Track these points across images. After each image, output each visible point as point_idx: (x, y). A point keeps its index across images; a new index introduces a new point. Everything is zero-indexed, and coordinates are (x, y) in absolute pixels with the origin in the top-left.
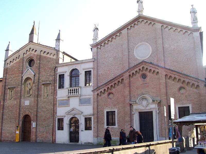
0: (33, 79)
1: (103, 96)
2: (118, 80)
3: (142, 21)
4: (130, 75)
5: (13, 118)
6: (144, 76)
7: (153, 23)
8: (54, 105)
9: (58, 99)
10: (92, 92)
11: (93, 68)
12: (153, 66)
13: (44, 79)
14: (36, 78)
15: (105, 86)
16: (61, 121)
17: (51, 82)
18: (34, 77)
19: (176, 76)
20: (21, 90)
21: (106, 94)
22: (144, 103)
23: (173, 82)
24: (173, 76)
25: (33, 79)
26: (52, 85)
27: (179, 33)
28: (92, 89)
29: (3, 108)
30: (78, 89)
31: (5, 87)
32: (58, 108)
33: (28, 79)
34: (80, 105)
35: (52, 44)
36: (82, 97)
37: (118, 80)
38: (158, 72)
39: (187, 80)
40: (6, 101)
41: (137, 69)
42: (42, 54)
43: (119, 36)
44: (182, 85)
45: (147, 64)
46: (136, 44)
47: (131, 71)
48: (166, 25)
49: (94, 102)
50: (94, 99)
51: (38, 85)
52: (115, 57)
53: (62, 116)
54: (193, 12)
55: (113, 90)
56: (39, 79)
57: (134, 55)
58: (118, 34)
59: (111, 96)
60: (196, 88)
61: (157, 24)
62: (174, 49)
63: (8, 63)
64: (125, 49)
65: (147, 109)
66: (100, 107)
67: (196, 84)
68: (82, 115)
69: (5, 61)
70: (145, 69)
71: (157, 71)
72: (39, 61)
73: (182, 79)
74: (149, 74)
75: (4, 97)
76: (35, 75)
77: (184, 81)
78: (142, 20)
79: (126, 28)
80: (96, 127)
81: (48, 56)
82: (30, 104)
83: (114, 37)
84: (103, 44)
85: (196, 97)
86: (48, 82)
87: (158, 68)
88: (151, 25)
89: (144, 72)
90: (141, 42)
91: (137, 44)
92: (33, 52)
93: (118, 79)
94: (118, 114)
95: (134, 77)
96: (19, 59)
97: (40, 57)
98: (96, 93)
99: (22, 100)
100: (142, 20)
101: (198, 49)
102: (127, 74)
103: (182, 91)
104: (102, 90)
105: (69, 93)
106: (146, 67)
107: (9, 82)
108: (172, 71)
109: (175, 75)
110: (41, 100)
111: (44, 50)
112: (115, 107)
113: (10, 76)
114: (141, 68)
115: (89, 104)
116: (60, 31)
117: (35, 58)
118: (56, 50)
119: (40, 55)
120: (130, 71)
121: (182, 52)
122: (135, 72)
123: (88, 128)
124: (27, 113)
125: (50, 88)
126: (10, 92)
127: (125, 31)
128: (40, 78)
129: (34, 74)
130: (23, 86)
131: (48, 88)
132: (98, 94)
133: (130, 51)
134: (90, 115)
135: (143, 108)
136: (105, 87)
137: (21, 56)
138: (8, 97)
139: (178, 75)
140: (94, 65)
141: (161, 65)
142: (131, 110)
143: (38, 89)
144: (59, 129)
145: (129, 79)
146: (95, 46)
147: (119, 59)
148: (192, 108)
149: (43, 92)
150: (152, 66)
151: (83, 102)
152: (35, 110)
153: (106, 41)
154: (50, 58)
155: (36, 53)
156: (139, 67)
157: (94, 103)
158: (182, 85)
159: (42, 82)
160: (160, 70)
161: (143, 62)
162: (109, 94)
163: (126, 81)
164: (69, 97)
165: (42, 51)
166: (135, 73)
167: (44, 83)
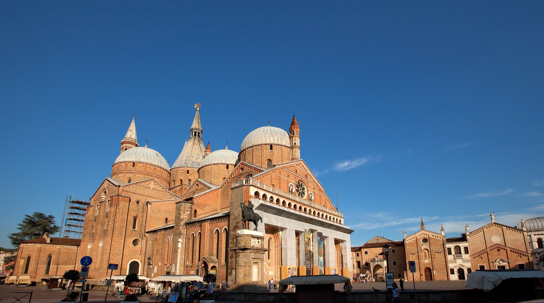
0: (429, 250)
6: (499, 250)
7: (501, 226)
11: (469, 246)
19: (516, 251)
41: (495, 247)
72: (431, 241)
73: (519, 253)
98: (473, 257)
124: (428, 266)
160: (507, 248)
161: (497, 244)
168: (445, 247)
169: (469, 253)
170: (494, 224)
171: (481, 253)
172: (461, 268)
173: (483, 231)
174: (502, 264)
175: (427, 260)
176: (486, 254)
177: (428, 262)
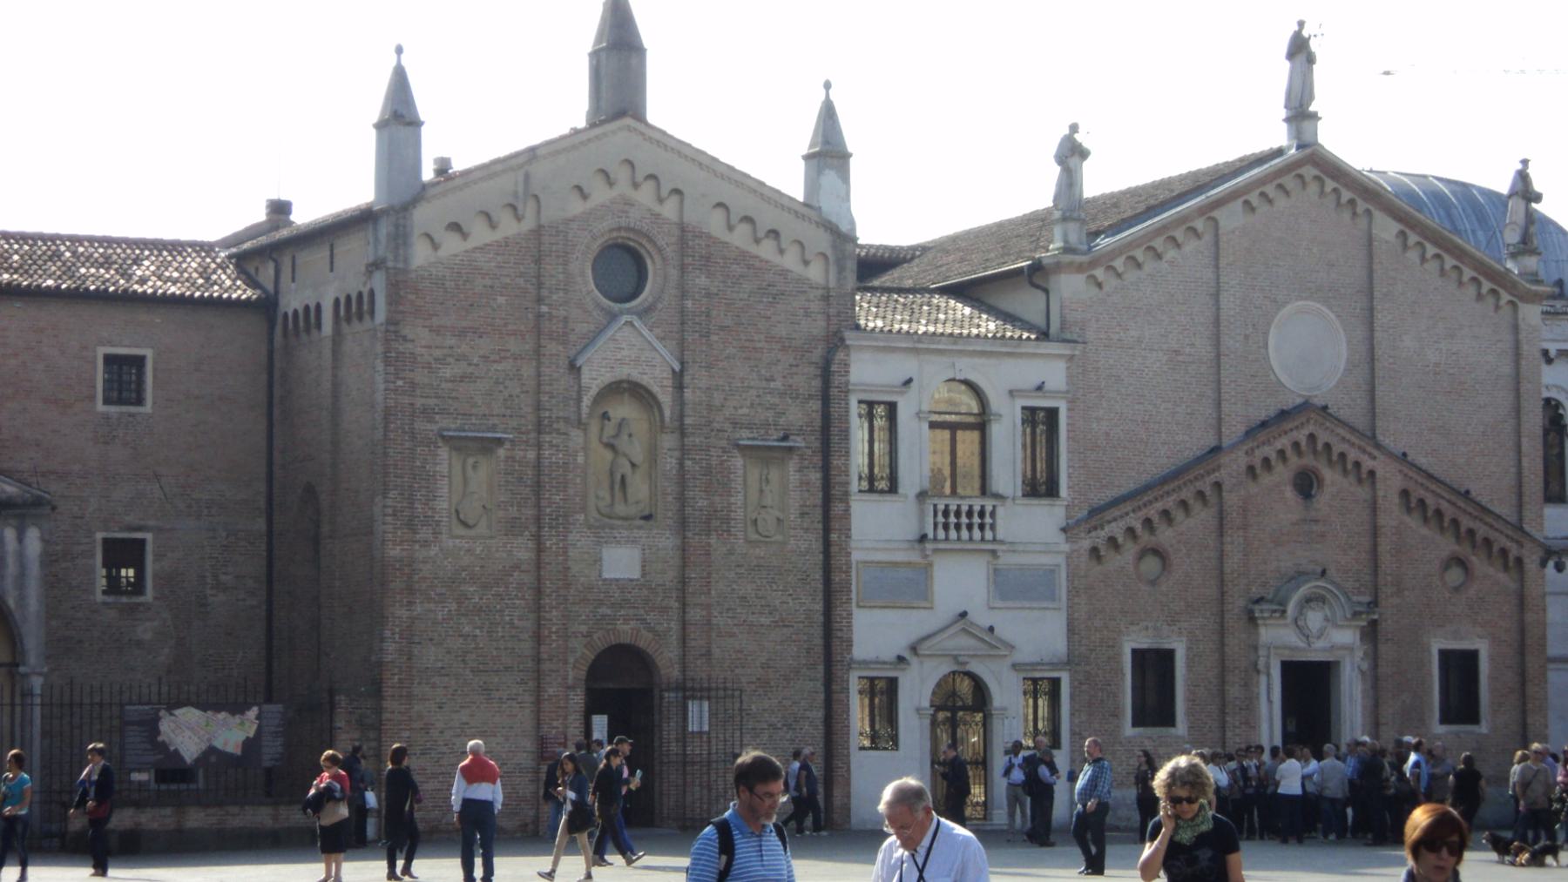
0: (666, 399)
2: (1199, 485)
3: (1317, 178)
4: (1251, 469)
5: (507, 669)
6: (1306, 484)
7: (1361, 206)
9: (856, 556)
10: (1062, 537)
11: (1072, 402)
12: (1353, 439)
13: (745, 411)
14: (688, 394)
15: (1134, 511)
16: (884, 695)
18: (679, 387)
19: (1444, 506)
22: (1314, 619)
23: (1425, 531)
25: (666, 399)
26: (802, 458)
32: (855, 611)
37: (1199, 485)
40: (424, 533)
41: (1284, 442)
44: (1456, 548)
46: (1275, 301)
47: (1258, 447)
48: (1418, 234)
49: (1073, 592)
50: (1071, 577)
52: (1177, 352)
55: (1165, 536)
57: (1267, 358)
59: (1151, 565)
61: (1379, 216)
62: (1437, 365)
68: (1009, 661)
72: (702, 281)
73: (1466, 523)
74: (1329, 475)
78: (1315, 172)
79: (1240, 201)
81: (766, 250)
82: (644, 575)
85: (1504, 610)
87: (1376, 453)
89: (1308, 461)
91: (1285, 303)
94: (1190, 666)
95: (1266, 480)
98: (1086, 544)
99: (580, 541)
104: (1116, 530)
106: (1323, 437)
107: (444, 385)
108: (1430, 477)
109: (1441, 501)
110: (731, 552)
111: (742, 203)
112: (1175, 628)
114: (1301, 436)
120: (1252, 449)
122: (1273, 456)
124: (625, 631)
125: (794, 477)
131: (774, 474)
132: (1094, 551)
133: (1247, 332)
134: (1054, 666)
135: (1302, 645)
136: (1132, 515)
139: (1449, 501)
140: (1070, 378)
141: (1387, 441)
148: (1492, 658)
149: (738, 499)
150: (1348, 436)
154: (784, 273)
155: (669, 210)
156: (1291, 430)
157: (1076, 600)
159: (727, 426)
160: (1382, 467)
161: (1305, 407)
166: (1273, 463)
168: (836, 380)
169: (1063, 492)
170: (1309, 171)
171: (1169, 503)
173: (1208, 238)
174: (1319, 644)
175: (634, 542)
176: (1202, 517)
177: (636, 574)
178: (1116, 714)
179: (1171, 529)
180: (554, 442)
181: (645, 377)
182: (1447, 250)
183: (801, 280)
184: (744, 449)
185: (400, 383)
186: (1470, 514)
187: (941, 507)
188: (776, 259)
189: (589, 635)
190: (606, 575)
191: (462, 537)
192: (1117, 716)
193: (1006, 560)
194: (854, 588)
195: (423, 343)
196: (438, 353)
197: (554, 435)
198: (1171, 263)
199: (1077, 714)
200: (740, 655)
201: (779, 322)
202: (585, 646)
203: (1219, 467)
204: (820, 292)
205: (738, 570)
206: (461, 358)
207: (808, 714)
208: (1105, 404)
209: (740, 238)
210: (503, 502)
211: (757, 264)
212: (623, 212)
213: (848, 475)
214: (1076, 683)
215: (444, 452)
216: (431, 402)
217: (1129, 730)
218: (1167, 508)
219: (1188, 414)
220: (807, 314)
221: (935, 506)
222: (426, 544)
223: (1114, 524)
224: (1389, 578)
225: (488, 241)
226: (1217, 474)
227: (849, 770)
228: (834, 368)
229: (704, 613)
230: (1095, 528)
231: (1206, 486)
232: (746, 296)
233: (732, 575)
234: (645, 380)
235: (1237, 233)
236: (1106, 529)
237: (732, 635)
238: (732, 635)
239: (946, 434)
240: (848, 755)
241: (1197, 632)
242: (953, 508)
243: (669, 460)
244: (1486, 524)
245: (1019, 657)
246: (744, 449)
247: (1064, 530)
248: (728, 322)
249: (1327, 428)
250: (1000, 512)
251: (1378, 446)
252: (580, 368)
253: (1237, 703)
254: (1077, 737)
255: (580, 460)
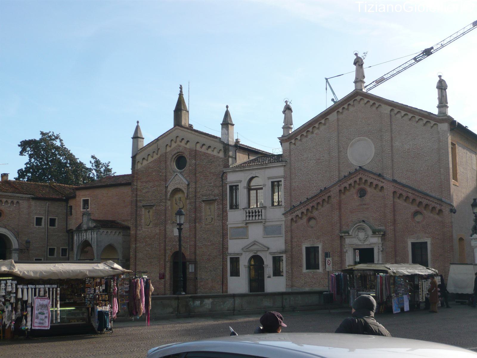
0: (185, 191)
1: (300, 222)
3: (361, 99)
4: (340, 191)
6: (362, 193)
7: (377, 104)
8: (224, 236)
9: (229, 226)
10: (283, 216)
11: (285, 177)
13: (205, 192)
15: (304, 207)
16: (235, 261)
17: (217, 197)
18: (188, 188)
19: (410, 195)
20: (165, 210)
21: (305, 219)
22: (362, 235)
23: (405, 204)
24: (404, 194)
25: (185, 191)
27: (418, 123)
28: (282, 210)
29: (136, 240)
30: (262, 210)
31: (136, 205)
32: (229, 240)
33: (177, 191)
34: (265, 237)
35: (217, 132)
36: (267, 224)
38: (382, 187)
39: (425, 202)
40: (139, 228)
41: (351, 181)
42: (198, 147)
43: (325, 124)
44: (418, 208)
45: (366, 174)
47: (343, 184)
48: (398, 109)
49: (286, 232)
50: (286, 227)
51: (195, 202)
52: (319, 159)
53: (238, 254)
54: (442, 86)
55: (315, 213)
56: (196, 192)
57: (347, 157)
58: (323, 121)
59: (312, 222)
60: (438, 214)
61: (383, 106)
62: (408, 149)
63: (138, 162)
64: (334, 147)
65: (366, 245)
66: (296, 240)
67: (438, 207)
69: (134, 158)
70: (363, 181)
71: (381, 184)
72: (194, 161)
74: (369, 189)
75: (136, 221)
76: (188, 185)
77: (420, 203)
78: (361, 97)
79: (336, 112)
80: (290, 272)
81: (209, 151)
83: (317, 125)
84: (299, 137)
85: (437, 228)
86: (212, 197)
87: (383, 181)
88: (374, 108)
89: (362, 186)
90: (359, 137)
91: (353, 139)
92: (183, 144)
93: (323, 195)
95: (347, 193)
96: (159, 156)
97: (195, 154)
98: (290, 218)
100: (361, 97)
101: (443, 151)
102: (336, 189)
103: (419, 218)
104: (299, 213)
105: (246, 216)
110: (201, 227)
113: (144, 184)
114: (357, 179)
115: (279, 236)
116: (227, 107)
117: (187, 155)
118: (223, 143)
119: (196, 150)
120: (341, 185)
121: (420, 155)
122: (348, 186)
123: (277, 272)
125: (216, 207)
126: (147, 213)
127: (333, 117)
128: (198, 190)
129: (187, 183)
130: (169, 203)
131: (212, 207)
132: (292, 219)
134: (281, 253)
137: (162, 151)
138: (143, 221)
139: (412, 193)
140: (285, 171)
141: (388, 177)
142: (342, 246)
143: (195, 208)
144: (232, 275)
145: (340, 197)
146: (286, 139)
147: (324, 163)
149: (203, 214)
151: (269, 231)
152: (192, 243)
153: (304, 131)
154: (214, 156)
155: (188, 146)
158: (418, 208)
159: (201, 196)
160: (386, 185)
162: (310, 219)
163: (334, 200)
164: (247, 223)
165: (198, 143)
166: (348, 188)
167: (205, 198)
172: (259, 254)
178: (301, 266)
179: (317, 211)
180: (163, 204)
181: (181, 187)
182: (409, 112)
183: (218, 157)
184: (203, 201)
185: (134, 195)
186: (420, 197)
187: (247, 211)
188: (212, 153)
189: (171, 249)
190: (174, 235)
191: (146, 228)
192: (301, 266)
193: (267, 224)
194: (228, 234)
195: (140, 186)
196: (142, 187)
197: (162, 203)
198: (316, 134)
199: (287, 266)
200: (203, 253)
201: (213, 169)
202: (170, 252)
203: (330, 191)
204: (222, 160)
205: (203, 231)
206: (147, 188)
207: (219, 267)
208: (297, 178)
209: (204, 150)
210: (154, 219)
211: (208, 155)
212: (179, 148)
213: (227, 205)
214: (287, 258)
215: (143, 209)
216: (140, 198)
217: (304, 270)
218: (313, 205)
219: (322, 177)
220: (219, 166)
221: (246, 211)
222: (140, 230)
223: (298, 211)
224: (389, 220)
225: (152, 160)
226: (329, 194)
227: (227, 283)
228: (224, 178)
229: (193, 243)
230: (292, 213)
231: (326, 197)
232: (205, 164)
233: (201, 233)
234: (181, 187)
235: (335, 121)
236: (295, 213)
237: (202, 248)
238: (202, 248)
239: (255, 191)
240: (227, 278)
241: (326, 241)
242: (251, 211)
243: (188, 206)
244: (427, 199)
245: (271, 251)
246: (203, 201)
247: (283, 214)
248: (201, 171)
249: (366, 175)
250: (263, 211)
251: (384, 179)
252: (168, 186)
253: (337, 262)
254: (287, 273)
255: (169, 208)
